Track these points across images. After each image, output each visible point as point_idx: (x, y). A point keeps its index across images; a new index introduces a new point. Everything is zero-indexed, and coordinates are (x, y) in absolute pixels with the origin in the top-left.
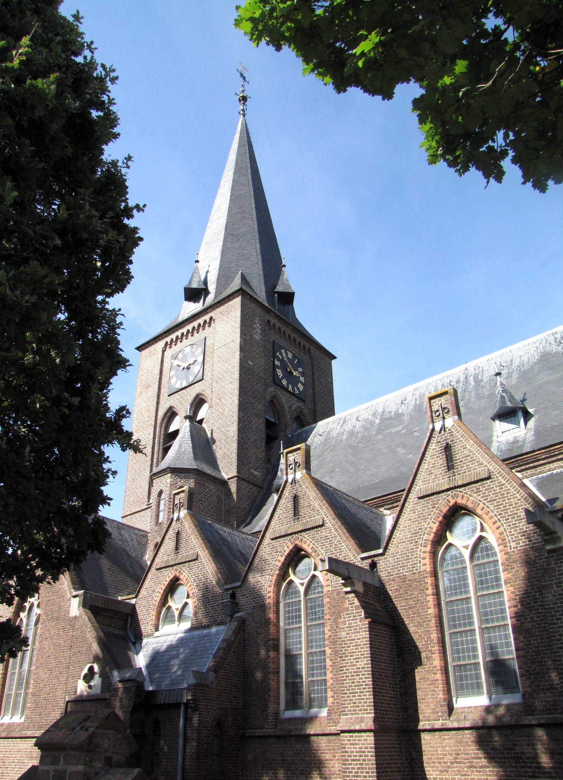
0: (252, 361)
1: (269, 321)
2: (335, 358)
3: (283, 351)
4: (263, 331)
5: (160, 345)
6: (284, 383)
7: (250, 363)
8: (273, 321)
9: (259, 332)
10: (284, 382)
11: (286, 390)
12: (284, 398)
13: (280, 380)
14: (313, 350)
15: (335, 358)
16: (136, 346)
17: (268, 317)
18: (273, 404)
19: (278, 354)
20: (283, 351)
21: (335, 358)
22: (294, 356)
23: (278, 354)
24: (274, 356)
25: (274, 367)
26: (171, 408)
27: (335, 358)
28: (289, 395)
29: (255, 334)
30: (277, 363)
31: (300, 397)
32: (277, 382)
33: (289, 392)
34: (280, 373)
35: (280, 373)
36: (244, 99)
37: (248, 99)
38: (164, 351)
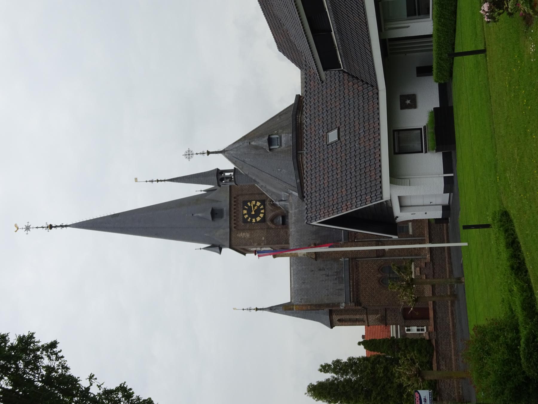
0: (262, 238)
1: (235, 227)
4: (243, 230)
7: (263, 239)
9: (244, 234)
10: (262, 215)
11: (264, 213)
12: (269, 216)
13: (262, 218)
17: (233, 229)
19: (249, 220)
23: (249, 220)
25: (256, 222)
28: (266, 212)
29: (247, 237)
32: (263, 220)
33: (265, 211)
34: (258, 219)
35: (258, 219)
36: (51, 227)
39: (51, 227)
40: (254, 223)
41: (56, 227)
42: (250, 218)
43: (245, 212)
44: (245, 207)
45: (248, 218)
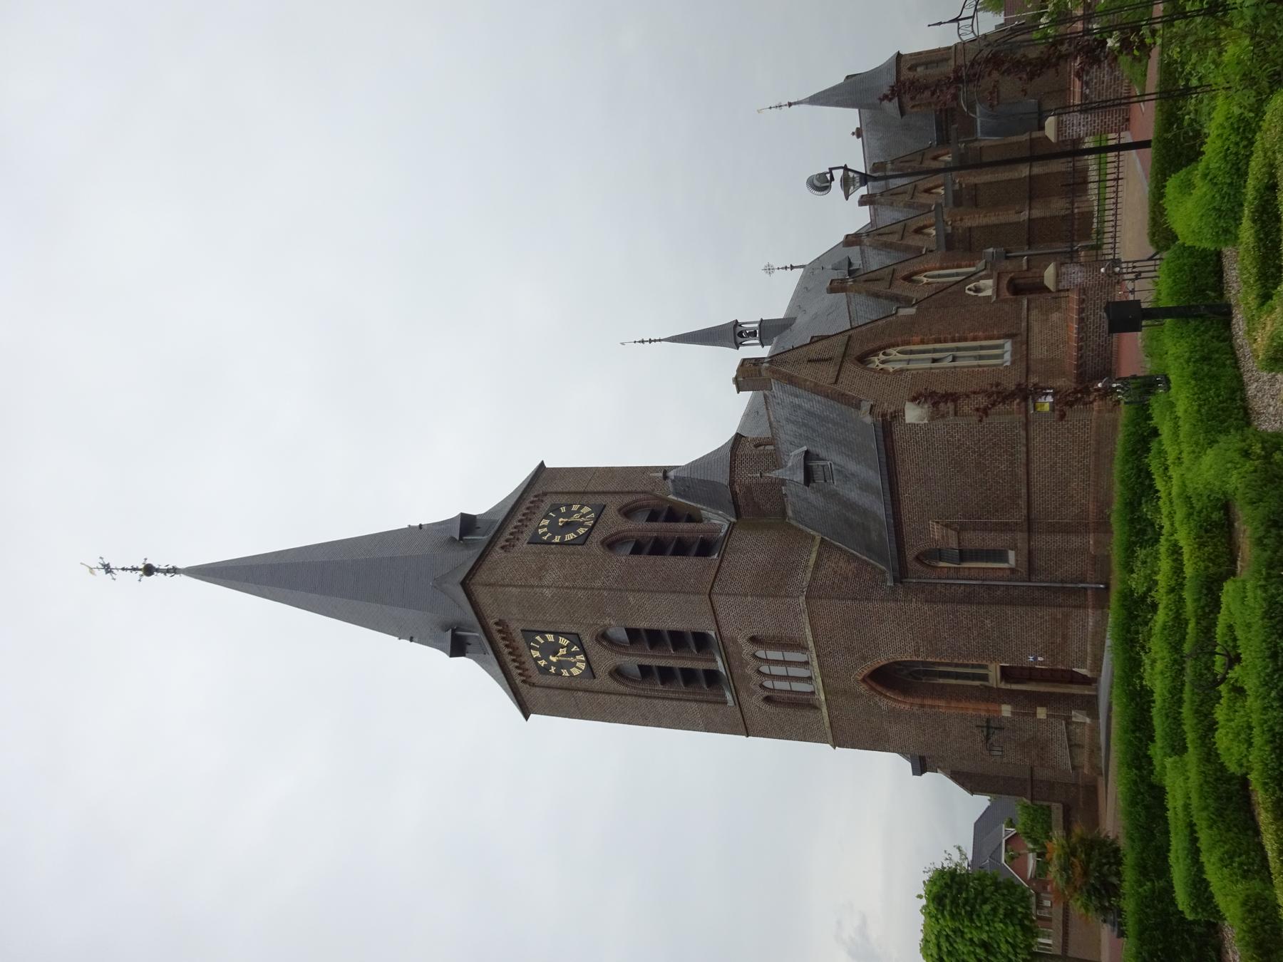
2: (542, 463)
3: (540, 531)
5: (524, 688)
6: (583, 532)
8: (502, 542)
10: (582, 531)
13: (579, 536)
14: (538, 489)
15: (542, 464)
16: (523, 719)
18: (611, 544)
19: (545, 538)
20: (540, 531)
21: (542, 464)
22: (546, 517)
23: (545, 538)
24: (549, 543)
25: (562, 543)
26: (611, 674)
27: (542, 462)
28: (597, 525)
30: (557, 539)
31: (600, 511)
32: (583, 540)
33: (594, 525)
36: (149, 570)
37: (148, 562)
38: (534, 685)
39: (149, 570)
40: (556, 544)
41: (158, 570)
42: (545, 529)
43: (546, 522)
44: (551, 514)
45: (545, 534)
